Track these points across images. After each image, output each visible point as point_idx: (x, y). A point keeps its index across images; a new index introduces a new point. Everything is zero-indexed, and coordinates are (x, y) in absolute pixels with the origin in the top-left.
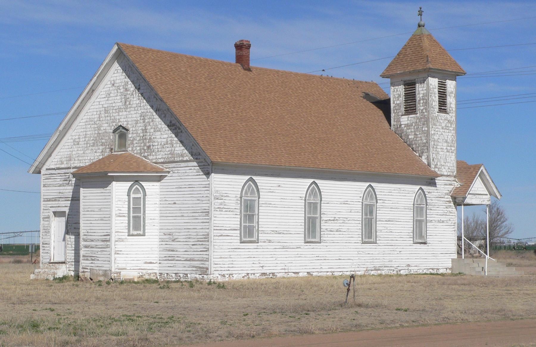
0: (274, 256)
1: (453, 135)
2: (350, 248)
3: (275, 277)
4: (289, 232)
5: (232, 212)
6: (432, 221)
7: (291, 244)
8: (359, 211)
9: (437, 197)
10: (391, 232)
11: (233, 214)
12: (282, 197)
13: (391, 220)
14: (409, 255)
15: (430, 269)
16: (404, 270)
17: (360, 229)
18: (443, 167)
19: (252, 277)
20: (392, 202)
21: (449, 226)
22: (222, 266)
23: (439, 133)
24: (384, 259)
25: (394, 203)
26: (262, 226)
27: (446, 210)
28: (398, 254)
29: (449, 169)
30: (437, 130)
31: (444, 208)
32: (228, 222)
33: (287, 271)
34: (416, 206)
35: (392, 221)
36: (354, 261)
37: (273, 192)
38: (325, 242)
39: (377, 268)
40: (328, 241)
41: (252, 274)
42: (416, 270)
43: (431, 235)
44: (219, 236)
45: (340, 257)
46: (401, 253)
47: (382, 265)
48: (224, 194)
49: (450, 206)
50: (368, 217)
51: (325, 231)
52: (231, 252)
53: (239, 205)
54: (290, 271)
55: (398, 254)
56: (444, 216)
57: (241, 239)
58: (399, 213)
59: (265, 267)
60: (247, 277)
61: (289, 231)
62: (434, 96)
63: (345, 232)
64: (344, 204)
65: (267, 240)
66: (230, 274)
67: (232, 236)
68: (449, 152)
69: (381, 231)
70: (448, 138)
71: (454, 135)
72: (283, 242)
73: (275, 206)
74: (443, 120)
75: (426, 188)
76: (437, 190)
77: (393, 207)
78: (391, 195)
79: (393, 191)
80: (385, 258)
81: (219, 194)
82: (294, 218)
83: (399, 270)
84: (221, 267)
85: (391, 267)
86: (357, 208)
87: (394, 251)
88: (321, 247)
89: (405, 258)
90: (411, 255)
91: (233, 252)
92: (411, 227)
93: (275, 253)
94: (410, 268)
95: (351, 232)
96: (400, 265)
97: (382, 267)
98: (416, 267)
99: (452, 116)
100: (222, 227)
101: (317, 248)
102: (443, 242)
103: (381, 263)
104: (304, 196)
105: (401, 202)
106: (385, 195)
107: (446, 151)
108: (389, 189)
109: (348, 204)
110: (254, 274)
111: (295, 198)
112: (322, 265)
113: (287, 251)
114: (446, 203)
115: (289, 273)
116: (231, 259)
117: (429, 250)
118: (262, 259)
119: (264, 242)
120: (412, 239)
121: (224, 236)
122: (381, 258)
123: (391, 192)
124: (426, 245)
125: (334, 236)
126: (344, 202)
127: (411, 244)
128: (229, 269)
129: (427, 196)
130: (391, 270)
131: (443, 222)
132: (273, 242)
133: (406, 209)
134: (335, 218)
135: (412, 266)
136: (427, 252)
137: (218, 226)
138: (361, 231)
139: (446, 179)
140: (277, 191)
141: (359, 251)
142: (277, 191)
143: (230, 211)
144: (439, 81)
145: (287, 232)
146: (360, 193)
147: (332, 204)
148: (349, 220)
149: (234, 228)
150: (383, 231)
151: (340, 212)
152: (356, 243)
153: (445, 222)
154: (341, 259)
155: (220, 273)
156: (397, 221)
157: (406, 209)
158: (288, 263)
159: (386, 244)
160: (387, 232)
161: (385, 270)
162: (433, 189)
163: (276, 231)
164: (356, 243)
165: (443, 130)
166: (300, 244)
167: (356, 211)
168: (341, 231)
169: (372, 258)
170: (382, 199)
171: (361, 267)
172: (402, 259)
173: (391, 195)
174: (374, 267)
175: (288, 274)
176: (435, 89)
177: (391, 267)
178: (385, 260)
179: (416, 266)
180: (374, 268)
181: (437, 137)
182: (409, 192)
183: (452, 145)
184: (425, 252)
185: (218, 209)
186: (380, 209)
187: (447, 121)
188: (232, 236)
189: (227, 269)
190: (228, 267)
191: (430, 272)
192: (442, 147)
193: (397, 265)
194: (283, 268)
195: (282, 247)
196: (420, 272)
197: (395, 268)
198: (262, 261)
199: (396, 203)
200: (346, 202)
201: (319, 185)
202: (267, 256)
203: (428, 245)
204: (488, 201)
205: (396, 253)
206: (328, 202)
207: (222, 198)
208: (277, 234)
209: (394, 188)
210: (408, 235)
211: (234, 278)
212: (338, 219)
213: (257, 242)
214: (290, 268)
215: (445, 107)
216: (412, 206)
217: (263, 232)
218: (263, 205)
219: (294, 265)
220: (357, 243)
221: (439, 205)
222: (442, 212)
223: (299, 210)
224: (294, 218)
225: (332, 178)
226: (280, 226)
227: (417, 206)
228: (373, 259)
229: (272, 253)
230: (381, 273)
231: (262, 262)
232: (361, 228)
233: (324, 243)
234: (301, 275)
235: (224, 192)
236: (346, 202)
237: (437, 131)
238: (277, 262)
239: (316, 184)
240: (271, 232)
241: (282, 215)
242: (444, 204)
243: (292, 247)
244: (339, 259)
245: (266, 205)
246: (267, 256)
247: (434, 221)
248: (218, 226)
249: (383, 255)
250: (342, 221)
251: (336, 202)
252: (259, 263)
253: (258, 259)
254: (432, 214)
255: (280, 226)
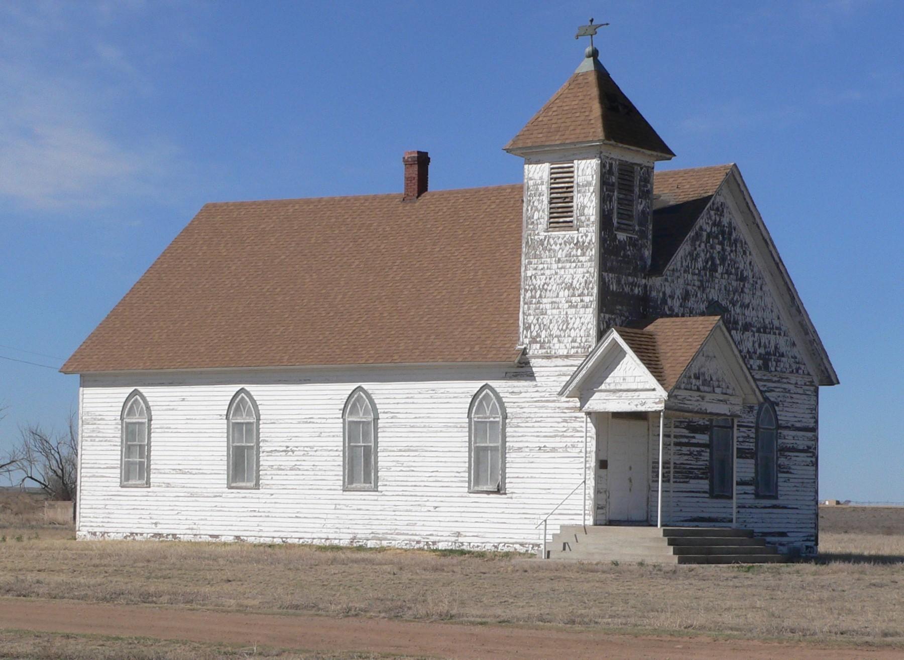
0: (176, 508)
1: (588, 272)
2: (320, 499)
3: (177, 540)
4: (201, 471)
5: (109, 441)
6: (520, 448)
7: (204, 491)
8: (338, 434)
9: (536, 402)
10: (413, 471)
11: (111, 445)
12: (188, 417)
13: (412, 448)
14: (459, 514)
15: (516, 543)
16: (447, 543)
17: (339, 465)
18: (556, 340)
19: (138, 538)
20: (414, 416)
21: (573, 459)
22: (92, 520)
23: (548, 272)
24: (396, 520)
25: (420, 418)
26: (157, 462)
27: (564, 427)
28: (430, 511)
29: (574, 341)
30: (541, 266)
31: (558, 422)
32: (103, 457)
33: (195, 532)
34: (475, 422)
35: (416, 451)
36: (328, 521)
37: (173, 410)
38: (268, 487)
39: (380, 536)
40: (274, 487)
41: (139, 535)
42: (476, 545)
43: (518, 477)
44: (90, 477)
45: (298, 513)
46: (437, 509)
47: (393, 531)
48: (97, 417)
49: (576, 417)
50: (361, 444)
51: (269, 469)
52: (108, 499)
53: (120, 432)
54: (202, 532)
55: (430, 511)
56: (558, 439)
57: (121, 483)
58: (434, 435)
59: (160, 524)
60: (132, 538)
61: (200, 469)
62: (539, 200)
63: (307, 470)
64: (306, 423)
65: (164, 483)
66: (105, 533)
67: (110, 477)
68: (576, 307)
69: (388, 469)
70: (573, 279)
71: (592, 270)
72: (190, 487)
73: (176, 430)
74: (561, 244)
75: (500, 386)
76: (536, 386)
77: (418, 425)
78: (413, 403)
79: (416, 396)
80: (398, 518)
81: (90, 417)
82: (209, 449)
83: (432, 542)
84: (91, 522)
85: (412, 535)
86: (333, 430)
87: (419, 505)
88: (261, 496)
89: (448, 519)
90: (463, 515)
91: (111, 499)
92: (465, 462)
93: (177, 503)
94: (461, 539)
95: (320, 470)
96: (434, 533)
97: (392, 534)
98: (476, 538)
99: (590, 233)
100: (94, 463)
101: (252, 498)
102: (552, 491)
103: (389, 527)
104: (225, 412)
105: (436, 416)
106: (398, 403)
107: (567, 305)
108: (407, 391)
109: (313, 423)
110: (141, 534)
111: (211, 417)
112: (261, 526)
113: (197, 501)
114: (565, 413)
115: (202, 536)
116: (107, 511)
117: (511, 506)
118: (156, 512)
119: (159, 486)
120: (467, 485)
121: (97, 477)
122: (389, 518)
123: (412, 398)
124: (504, 496)
125: (285, 477)
126: (306, 420)
127: (465, 495)
128: (104, 524)
129: (504, 400)
130: (449, 542)
131: (554, 450)
132: (173, 487)
133: (448, 427)
134: (288, 447)
135: (466, 536)
136: (507, 511)
137: (88, 463)
138: (342, 469)
139: (564, 364)
140: (180, 408)
141: (339, 505)
142: (180, 408)
143: (105, 441)
144: (552, 169)
145: (197, 471)
146: (339, 402)
147: (281, 423)
148: (316, 451)
149: (112, 466)
150: (393, 469)
151: (296, 437)
152: (331, 490)
153: (561, 450)
154: (300, 517)
155: (90, 530)
156: (426, 451)
157: (448, 427)
158: (199, 520)
159: (400, 493)
160: (402, 471)
161: (400, 540)
162: (524, 386)
163: (180, 470)
164: (331, 490)
165: (560, 265)
166: (220, 490)
167: (332, 434)
168: (300, 470)
169: (366, 517)
170: (389, 410)
171: (343, 533)
172: (439, 521)
173: (413, 403)
174: (372, 533)
175: (200, 538)
176: (543, 184)
177: (412, 535)
178: (397, 523)
179: (477, 536)
180: (372, 535)
181: (543, 281)
182: (456, 395)
183: (586, 292)
184: (500, 511)
185: (89, 439)
186: (385, 429)
187: (572, 245)
188: (110, 477)
189: (101, 525)
190: (102, 522)
191: (516, 549)
192: (554, 300)
193: (431, 533)
194: (191, 526)
195: (189, 495)
196: (486, 548)
197: (424, 538)
198: (154, 514)
199: (423, 418)
200: (309, 420)
201: (252, 393)
202: (162, 508)
203: (508, 495)
204: (656, 403)
205: (426, 509)
206: (273, 421)
207: (95, 422)
208: (180, 474)
209: (419, 390)
210: (455, 477)
211: (112, 538)
212: (295, 449)
213: (145, 486)
214: (202, 527)
215: (571, 216)
216: (467, 420)
217: (157, 471)
218: (157, 430)
219: (210, 523)
220: (334, 490)
221: (542, 417)
222: (551, 429)
223: (218, 435)
224: (209, 449)
225: (280, 381)
226: (185, 462)
227: (480, 420)
228: (370, 519)
229: (172, 504)
230: (389, 545)
231: (154, 516)
232: (341, 463)
233: (265, 489)
234: (223, 539)
235: (97, 413)
236: (309, 420)
237: (542, 269)
238: (181, 517)
239: (248, 394)
240: (171, 471)
241: (189, 444)
242: (557, 415)
243: (206, 495)
244: (297, 517)
245: (163, 430)
246: (162, 508)
247: (527, 450)
248: (88, 463)
249: (394, 513)
250: (303, 453)
251: (290, 421)
252: (151, 518)
253: (148, 512)
254: (522, 436)
255: (185, 462)
